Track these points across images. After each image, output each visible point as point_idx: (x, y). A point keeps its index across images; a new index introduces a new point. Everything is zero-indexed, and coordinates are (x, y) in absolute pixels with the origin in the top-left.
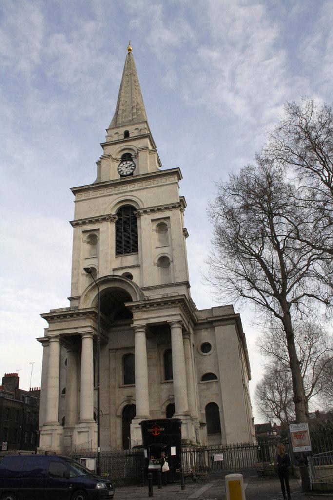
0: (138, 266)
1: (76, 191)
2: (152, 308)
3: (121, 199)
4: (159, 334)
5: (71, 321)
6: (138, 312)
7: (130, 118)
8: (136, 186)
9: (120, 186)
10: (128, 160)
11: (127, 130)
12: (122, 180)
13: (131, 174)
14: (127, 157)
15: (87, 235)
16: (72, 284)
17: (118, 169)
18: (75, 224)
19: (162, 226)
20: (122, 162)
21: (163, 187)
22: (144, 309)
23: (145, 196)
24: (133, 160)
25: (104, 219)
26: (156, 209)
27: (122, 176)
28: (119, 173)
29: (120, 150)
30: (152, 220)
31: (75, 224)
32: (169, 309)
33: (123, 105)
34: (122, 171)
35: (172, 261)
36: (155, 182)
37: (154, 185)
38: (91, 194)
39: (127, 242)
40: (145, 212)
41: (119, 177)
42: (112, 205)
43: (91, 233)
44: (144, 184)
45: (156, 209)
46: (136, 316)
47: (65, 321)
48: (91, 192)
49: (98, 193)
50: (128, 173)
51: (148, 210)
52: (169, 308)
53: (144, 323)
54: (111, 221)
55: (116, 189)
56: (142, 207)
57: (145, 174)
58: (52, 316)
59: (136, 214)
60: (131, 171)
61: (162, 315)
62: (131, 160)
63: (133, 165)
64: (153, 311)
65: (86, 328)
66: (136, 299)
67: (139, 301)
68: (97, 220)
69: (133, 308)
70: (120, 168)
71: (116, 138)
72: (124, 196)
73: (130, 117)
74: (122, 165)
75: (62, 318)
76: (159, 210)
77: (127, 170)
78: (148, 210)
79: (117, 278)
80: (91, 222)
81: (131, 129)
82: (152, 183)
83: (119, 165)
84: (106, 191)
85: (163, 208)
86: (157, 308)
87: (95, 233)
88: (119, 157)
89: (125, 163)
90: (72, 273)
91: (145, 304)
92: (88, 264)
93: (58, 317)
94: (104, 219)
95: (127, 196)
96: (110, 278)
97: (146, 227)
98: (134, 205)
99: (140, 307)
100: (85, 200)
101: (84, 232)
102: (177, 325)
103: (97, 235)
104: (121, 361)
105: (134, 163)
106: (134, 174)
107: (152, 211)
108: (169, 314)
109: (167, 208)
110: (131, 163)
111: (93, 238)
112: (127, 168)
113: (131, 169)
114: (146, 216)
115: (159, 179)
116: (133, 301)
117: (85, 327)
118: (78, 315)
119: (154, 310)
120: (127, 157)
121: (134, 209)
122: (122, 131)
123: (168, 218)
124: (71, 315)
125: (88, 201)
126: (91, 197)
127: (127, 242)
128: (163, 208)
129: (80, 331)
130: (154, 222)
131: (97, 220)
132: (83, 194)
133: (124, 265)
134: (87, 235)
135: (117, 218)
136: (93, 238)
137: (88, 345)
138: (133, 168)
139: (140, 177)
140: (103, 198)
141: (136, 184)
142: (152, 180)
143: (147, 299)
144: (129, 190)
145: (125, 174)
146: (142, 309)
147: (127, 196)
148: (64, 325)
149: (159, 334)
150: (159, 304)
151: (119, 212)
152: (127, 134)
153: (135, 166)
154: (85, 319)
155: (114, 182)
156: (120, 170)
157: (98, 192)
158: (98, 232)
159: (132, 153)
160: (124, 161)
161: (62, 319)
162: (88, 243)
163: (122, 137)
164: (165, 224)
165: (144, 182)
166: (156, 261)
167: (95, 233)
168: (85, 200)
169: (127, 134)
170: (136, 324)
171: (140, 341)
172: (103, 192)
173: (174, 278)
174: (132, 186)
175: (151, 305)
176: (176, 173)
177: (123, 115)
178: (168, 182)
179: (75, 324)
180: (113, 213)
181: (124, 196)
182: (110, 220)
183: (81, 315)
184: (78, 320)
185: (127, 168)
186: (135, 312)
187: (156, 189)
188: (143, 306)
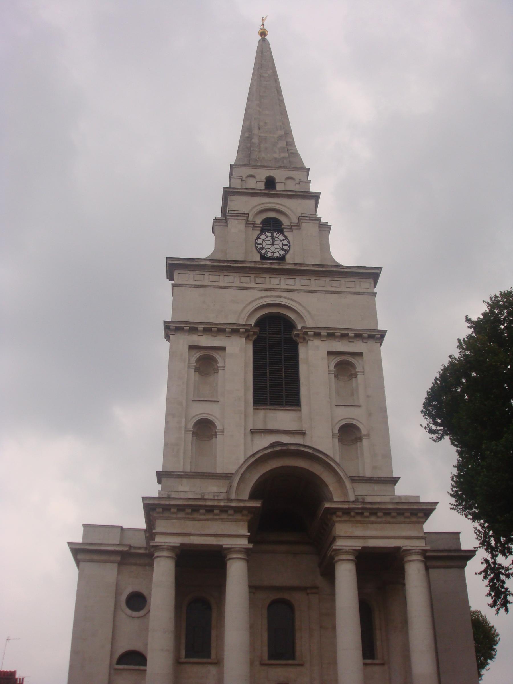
1: (176, 267)
2: (373, 519)
3: (268, 301)
4: (381, 571)
5: (207, 520)
6: (345, 522)
7: (276, 155)
8: (298, 283)
9: (267, 276)
10: (275, 230)
11: (272, 174)
12: (273, 267)
14: (272, 225)
15: (198, 354)
16: (166, 445)
17: (256, 244)
18: (171, 329)
19: (345, 367)
21: (349, 296)
22: (359, 518)
24: (286, 233)
26: (338, 333)
27: (263, 257)
28: (259, 250)
29: (260, 208)
30: (330, 353)
32: (403, 525)
33: (259, 129)
34: (263, 248)
35: (368, 436)
36: (335, 284)
37: (333, 289)
38: (208, 278)
40: (317, 335)
41: (258, 258)
42: (251, 308)
43: (207, 352)
44: (313, 283)
45: (338, 333)
47: (194, 519)
48: (207, 274)
49: (223, 280)
50: (276, 255)
51: (324, 333)
52: (404, 522)
53: (358, 544)
54: (247, 338)
55: (259, 280)
56: (310, 323)
57: (313, 265)
58: (169, 505)
59: (297, 335)
60: (282, 252)
61: (392, 534)
62: (282, 232)
63: (285, 242)
64: (375, 526)
65: (235, 539)
67: (353, 502)
68: (220, 330)
69: (339, 513)
70: (260, 241)
71: (251, 184)
72: (271, 296)
73: (275, 152)
74: (263, 237)
75: (189, 511)
76: (344, 336)
77: (273, 249)
78: (324, 333)
79: (308, 450)
81: (279, 175)
82: (326, 284)
83: (258, 237)
84: (237, 279)
85: (351, 335)
86: (384, 519)
87: (214, 354)
88: (258, 221)
89: (269, 234)
90: (167, 422)
91: (362, 508)
92: (200, 411)
93: (181, 508)
94: (235, 332)
95: (281, 297)
96: (293, 448)
97: (314, 362)
98: (292, 316)
99: (352, 514)
100: (195, 286)
101: (192, 348)
102: (165, 554)
103: (220, 362)
104: (265, 612)
105: (286, 238)
106: (289, 258)
107: (331, 335)
108: (404, 534)
109: (358, 336)
110: (281, 237)
111: (206, 362)
112: (273, 244)
113: (282, 249)
114: (317, 342)
115: (342, 280)
116: (335, 499)
117: (233, 535)
118: (224, 510)
119: (372, 523)
121: (290, 325)
122: (263, 174)
123: (360, 354)
124: (210, 510)
125: (202, 290)
126: (206, 283)
128: (351, 335)
129: (226, 542)
130: (332, 357)
131: (220, 330)
132: (191, 273)
133: (270, 427)
134: (198, 354)
135: (256, 330)
136: (206, 362)
138: (286, 248)
139: (308, 268)
140: (233, 291)
141: (298, 278)
142: (328, 279)
143: (361, 500)
144: (283, 286)
145: (269, 254)
146: (354, 517)
147: (281, 297)
148: (190, 526)
149: (381, 571)
150: (387, 513)
151: (260, 323)
152: (270, 183)
153: (288, 245)
154: (236, 520)
155: (258, 266)
156: (259, 246)
157: (222, 278)
158: (220, 352)
159: (285, 221)
160: (269, 230)
161: (188, 514)
162: (197, 370)
163: (262, 186)
164: (350, 365)
165: (313, 279)
166: (336, 431)
167: (214, 354)
168: (195, 286)
169: (270, 183)
170: (339, 544)
171: (346, 575)
172: (231, 279)
173: (375, 468)
174: (291, 282)
175: (374, 512)
176: (372, 275)
177: (262, 145)
178: (358, 289)
180: (252, 322)
181: (271, 296)
182: (246, 334)
183: (230, 512)
184: (222, 520)
185: (273, 244)
186: (341, 522)
187: (335, 296)
188: (357, 513)
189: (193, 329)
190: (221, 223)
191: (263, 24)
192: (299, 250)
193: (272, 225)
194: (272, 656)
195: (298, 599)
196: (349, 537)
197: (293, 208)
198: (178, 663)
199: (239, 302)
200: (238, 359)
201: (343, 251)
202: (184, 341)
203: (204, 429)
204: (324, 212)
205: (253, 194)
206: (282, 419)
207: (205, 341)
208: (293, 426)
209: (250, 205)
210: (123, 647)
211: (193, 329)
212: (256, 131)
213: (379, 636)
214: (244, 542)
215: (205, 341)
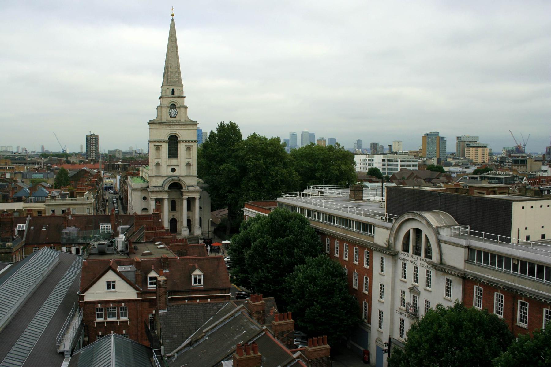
0: (178, 165)
13: (175, 117)
20: (171, 108)
25: (164, 141)
27: (171, 117)
31: (150, 141)
38: (158, 127)
44: (183, 127)
46: (184, 194)
53: (187, 197)
62: (175, 108)
76: (189, 142)
80: (158, 141)
94: (164, 141)
107: (186, 142)
109: (192, 142)
114: (182, 143)
117: (165, 196)
120: (173, 106)
129: (164, 197)
136: (158, 148)
148: (158, 194)
149: (191, 201)
152: (173, 91)
169: (173, 91)
170: (184, 197)
179: (162, 194)
189: (155, 141)
190: (159, 108)
191: (173, 15)
192: (181, 118)
193: (173, 106)
194: (172, 210)
195: (177, 200)
196: (186, 196)
197: (178, 101)
199: (164, 134)
200: (165, 147)
202: (152, 145)
204: (186, 102)
206: (174, 162)
207: (157, 144)
208: (176, 164)
209: (167, 102)
210: (143, 207)
211: (155, 141)
212: (170, 69)
213: (191, 206)
214: (167, 197)
215: (157, 144)
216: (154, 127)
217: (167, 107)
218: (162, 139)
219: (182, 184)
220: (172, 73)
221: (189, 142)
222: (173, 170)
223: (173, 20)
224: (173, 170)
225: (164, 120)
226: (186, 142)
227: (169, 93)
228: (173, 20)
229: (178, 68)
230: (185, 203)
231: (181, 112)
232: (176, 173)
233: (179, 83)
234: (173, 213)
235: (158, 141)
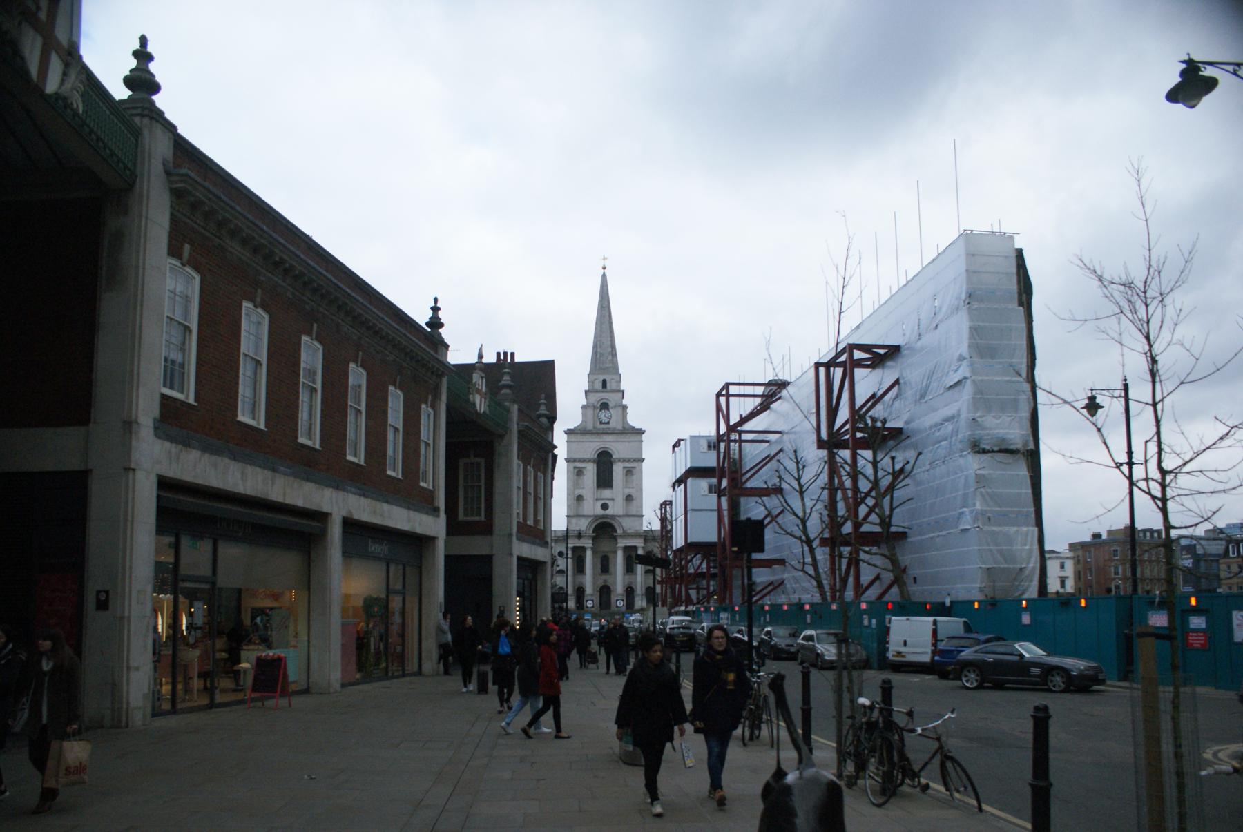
8: (610, 438)
14: (605, 406)
18: (568, 460)
19: (629, 472)
23: (618, 448)
25: (589, 461)
38: (579, 437)
39: (604, 480)
46: (619, 540)
66: (619, 532)
68: (584, 461)
76: (629, 461)
80: (580, 461)
92: (578, 492)
94: (589, 461)
97: (618, 470)
107: (624, 461)
111: (579, 472)
117: (587, 543)
121: (611, 456)
122: (602, 377)
127: (604, 480)
131: (584, 461)
136: (579, 472)
137: (589, 554)
152: (604, 382)
169: (604, 382)
176: (640, 432)
189: (575, 461)
192: (615, 424)
193: (605, 406)
195: (610, 555)
196: (622, 543)
197: (612, 398)
198: (574, 575)
199: (590, 448)
200: (591, 470)
201: (633, 420)
203: (580, 498)
205: (597, 391)
206: (606, 493)
209: (595, 398)
211: (575, 461)
216: (573, 438)
217: (595, 407)
218: (588, 456)
219: (616, 525)
220: (602, 355)
221: (629, 461)
222: (605, 507)
223: (604, 276)
224: (605, 507)
225: (590, 427)
226: (624, 461)
227: (598, 385)
228: (604, 276)
229: (613, 347)
230: (620, 555)
231: (615, 414)
232: (609, 512)
233: (615, 369)
234: (604, 577)
235: (580, 461)
